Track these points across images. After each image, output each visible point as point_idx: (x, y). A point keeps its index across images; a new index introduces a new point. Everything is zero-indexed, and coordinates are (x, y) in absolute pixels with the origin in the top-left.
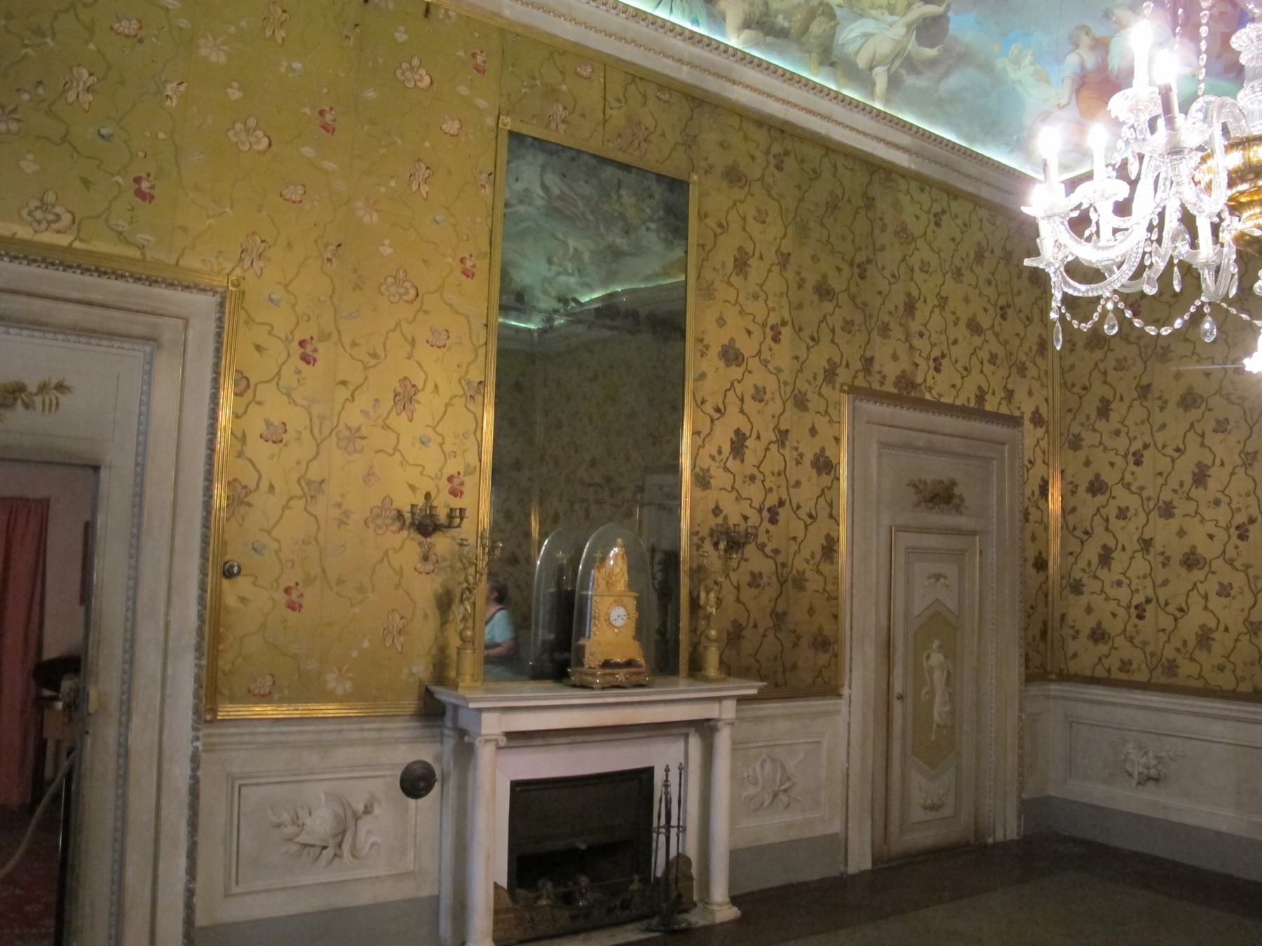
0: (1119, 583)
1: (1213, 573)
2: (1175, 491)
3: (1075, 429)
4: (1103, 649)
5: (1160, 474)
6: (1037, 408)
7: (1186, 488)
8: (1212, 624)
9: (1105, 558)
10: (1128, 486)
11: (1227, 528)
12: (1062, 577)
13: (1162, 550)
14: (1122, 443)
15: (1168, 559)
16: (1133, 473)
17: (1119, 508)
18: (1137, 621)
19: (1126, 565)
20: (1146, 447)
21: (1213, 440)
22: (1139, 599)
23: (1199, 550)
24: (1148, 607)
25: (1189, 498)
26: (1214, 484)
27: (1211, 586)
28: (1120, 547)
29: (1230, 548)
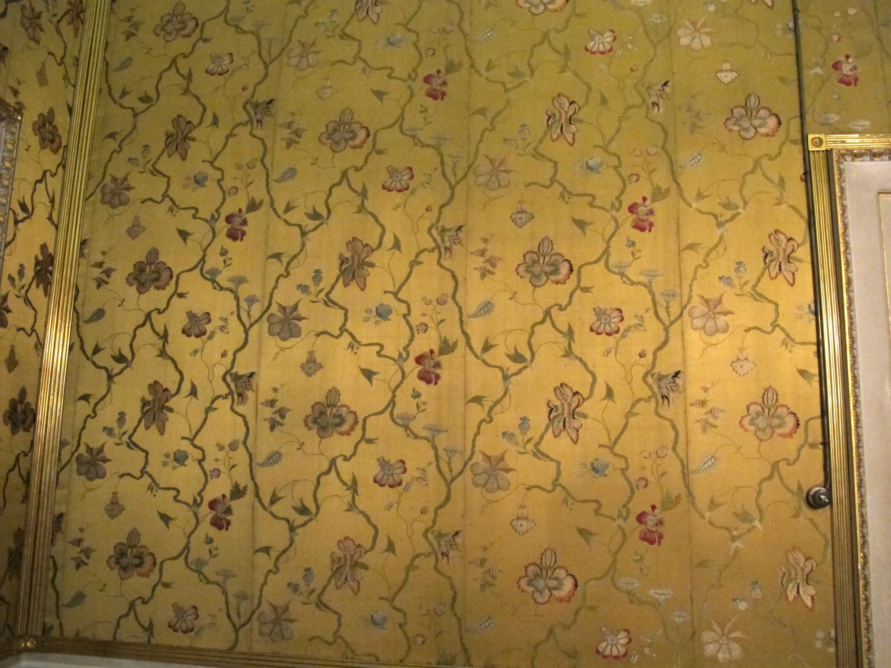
0: (180, 458)
1: (370, 441)
2: (304, 289)
3: (119, 168)
4: (138, 585)
5: (277, 256)
6: (51, 111)
7: (325, 284)
8: (364, 536)
9: (156, 407)
10: (212, 277)
11: (400, 359)
12: (63, 444)
13: (271, 396)
14: (207, 199)
15: (282, 413)
16: (224, 253)
17: (191, 316)
18: (213, 532)
20: (253, 206)
21: (385, 205)
22: (219, 488)
23: (345, 399)
25: (329, 302)
27: (365, 467)
28: (186, 388)
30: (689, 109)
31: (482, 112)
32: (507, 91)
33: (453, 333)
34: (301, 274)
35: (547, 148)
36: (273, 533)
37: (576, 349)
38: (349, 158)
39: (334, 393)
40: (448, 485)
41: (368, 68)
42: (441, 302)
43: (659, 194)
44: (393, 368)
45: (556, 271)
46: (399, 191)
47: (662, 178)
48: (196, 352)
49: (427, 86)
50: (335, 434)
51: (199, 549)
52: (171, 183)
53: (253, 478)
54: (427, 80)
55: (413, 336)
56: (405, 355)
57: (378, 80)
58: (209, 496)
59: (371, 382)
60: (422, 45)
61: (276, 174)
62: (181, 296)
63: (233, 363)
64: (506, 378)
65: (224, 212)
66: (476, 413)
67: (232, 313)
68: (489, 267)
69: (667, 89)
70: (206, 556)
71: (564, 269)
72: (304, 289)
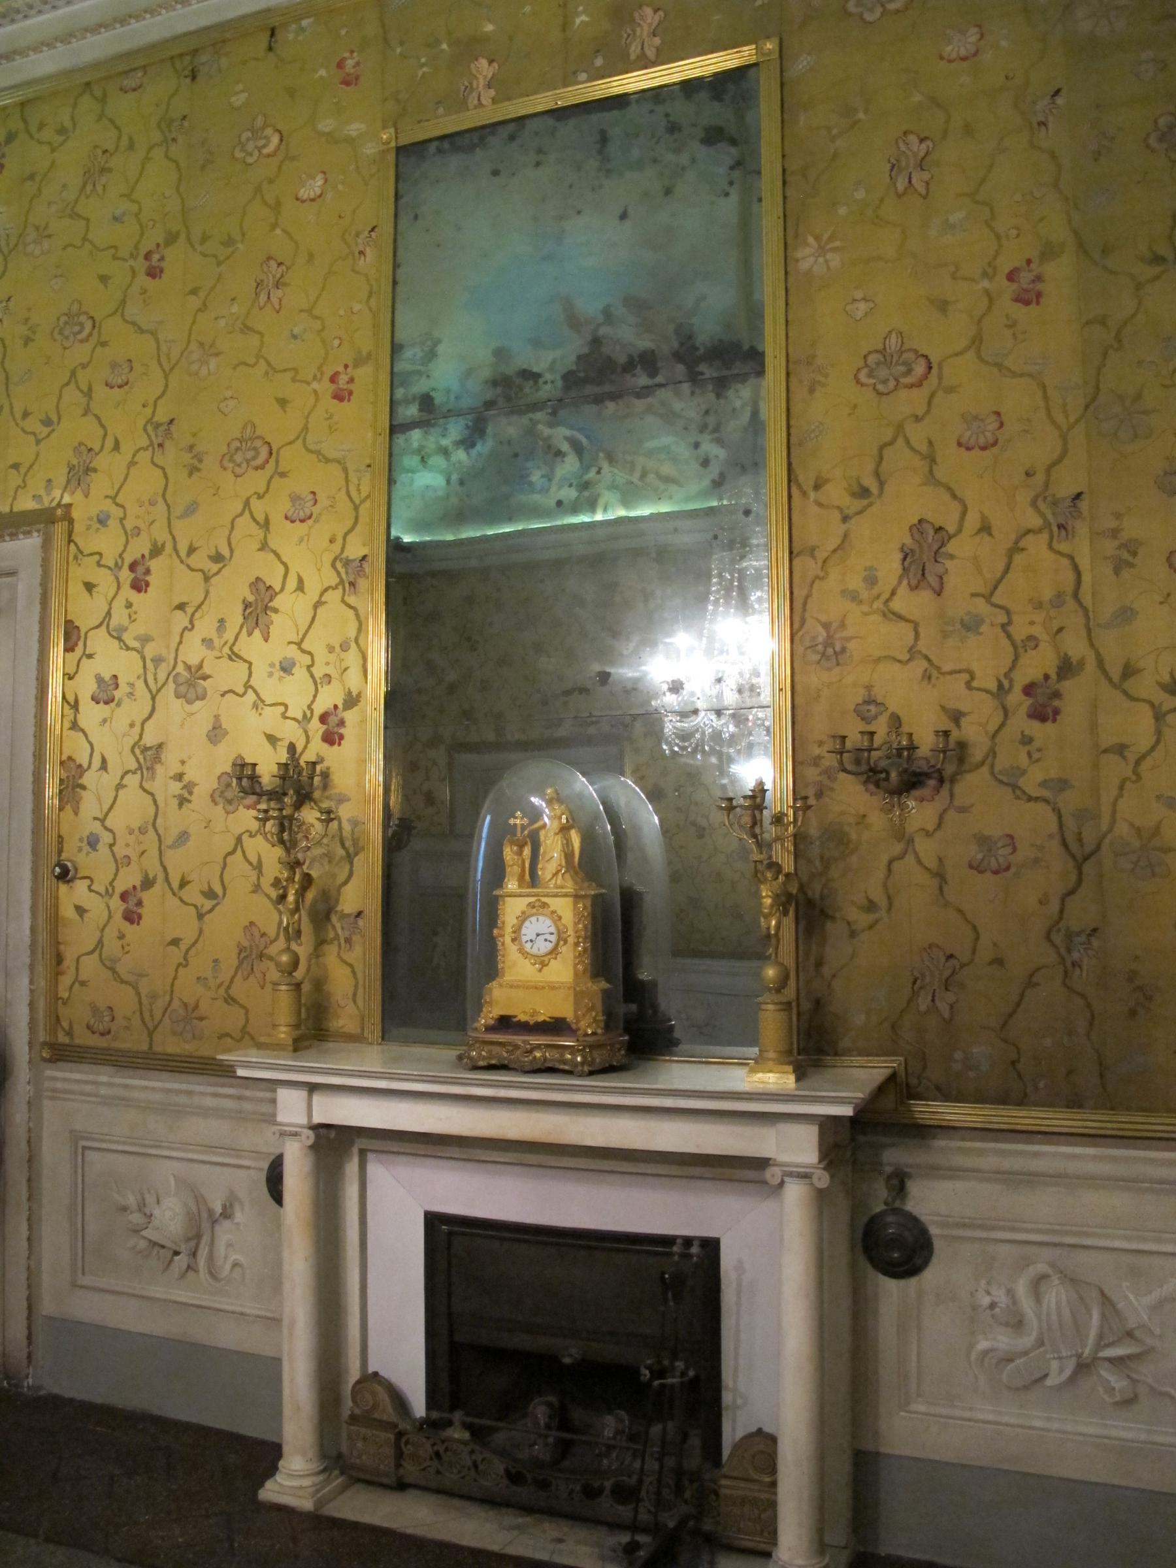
10: (118, 636)
16: (129, 605)
20: (156, 551)
21: (285, 538)
36: (184, 925)
48: (105, 721)
49: (334, 387)
50: (241, 808)
61: (178, 510)
62: (90, 656)
63: (141, 735)
65: (128, 559)
67: (138, 677)
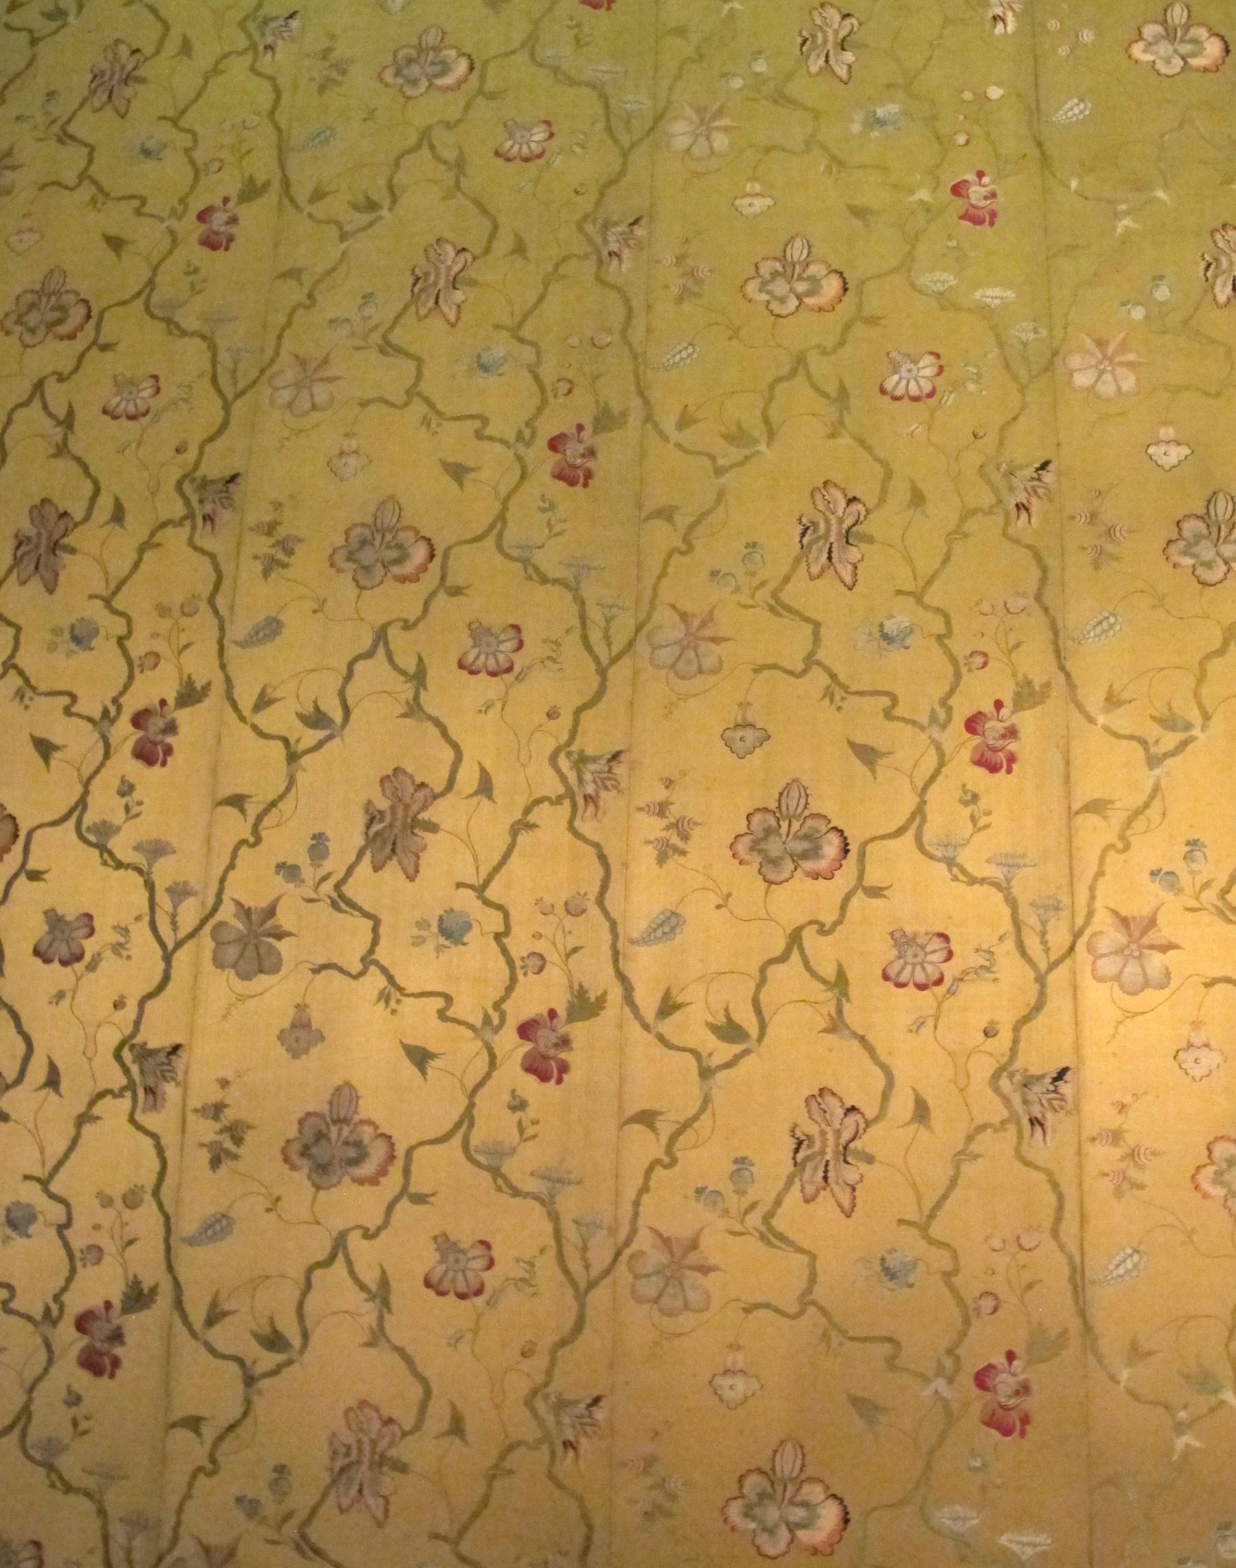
1: (419, 1199)
2: (289, 871)
5: (237, 801)
7: (335, 864)
8: (399, 1398)
10: (98, 839)
11: (489, 1025)
13: (216, 1095)
14: (95, 675)
15: (236, 1132)
16: (126, 789)
17: (55, 920)
18: (83, 1380)
19: (57, 1146)
20: (190, 695)
21: (460, 699)
22: (99, 1286)
23: (368, 1107)
24: (133, 1323)
25: (342, 902)
26: (446, 860)
27: (408, 1252)
29: (491, 1105)
30: (1093, 516)
31: (666, 513)
32: (719, 471)
33: (596, 974)
34: (285, 841)
35: (799, 592)
36: (209, 1388)
37: (852, 1015)
38: (393, 600)
39: (345, 1094)
40: (581, 1297)
41: (435, 416)
42: (574, 910)
43: (1028, 695)
44: (470, 1046)
45: (814, 852)
46: (493, 674)
47: (1035, 662)
48: (60, 995)
50: (346, 1179)
51: (50, 1418)
52: (22, 639)
53: (170, 1268)
54: (555, 444)
55: (513, 979)
56: (496, 1021)
57: (454, 441)
58: (76, 1303)
59: (424, 1073)
60: (548, 372)
61: (239, 628)
62: (35, 876)
63: (137, 1024)
64: (706, 1073)
66: (643, 1146)
67: (138, 918)
68: (675, 840)
69: (1048, 477)
70: (66, 1433)
71: (831, 848)
72: (289, 871)
